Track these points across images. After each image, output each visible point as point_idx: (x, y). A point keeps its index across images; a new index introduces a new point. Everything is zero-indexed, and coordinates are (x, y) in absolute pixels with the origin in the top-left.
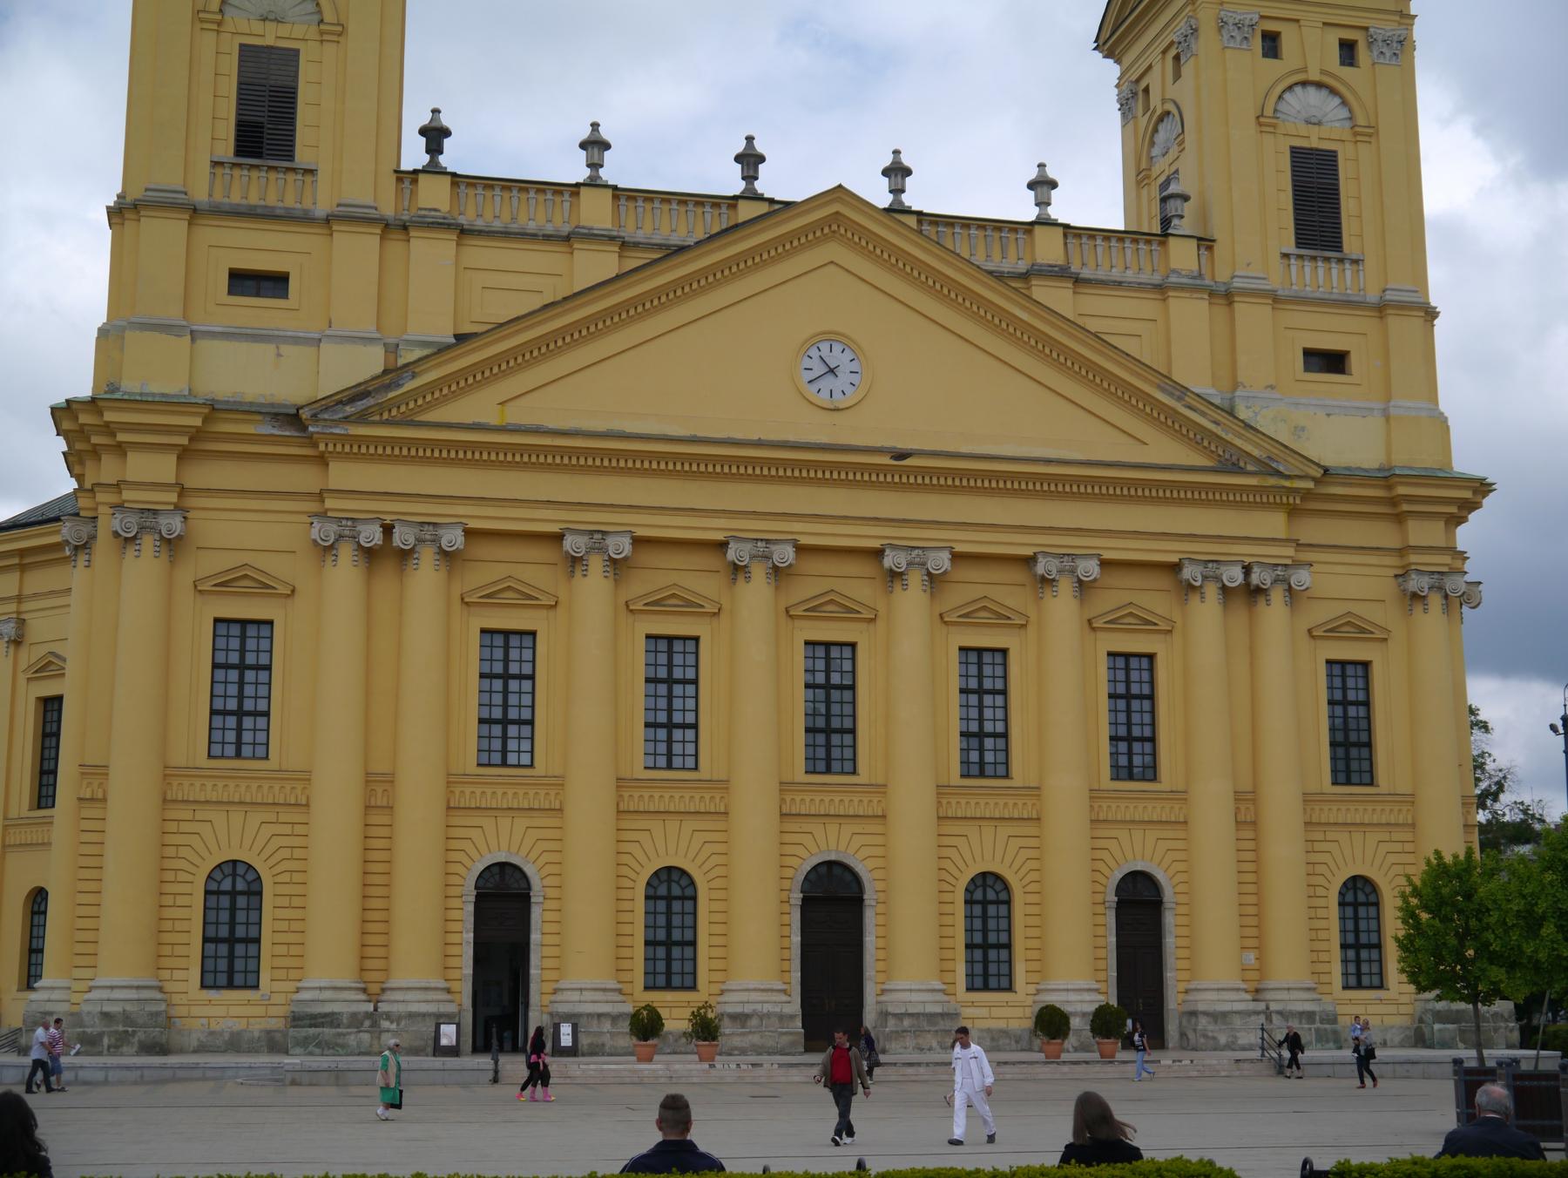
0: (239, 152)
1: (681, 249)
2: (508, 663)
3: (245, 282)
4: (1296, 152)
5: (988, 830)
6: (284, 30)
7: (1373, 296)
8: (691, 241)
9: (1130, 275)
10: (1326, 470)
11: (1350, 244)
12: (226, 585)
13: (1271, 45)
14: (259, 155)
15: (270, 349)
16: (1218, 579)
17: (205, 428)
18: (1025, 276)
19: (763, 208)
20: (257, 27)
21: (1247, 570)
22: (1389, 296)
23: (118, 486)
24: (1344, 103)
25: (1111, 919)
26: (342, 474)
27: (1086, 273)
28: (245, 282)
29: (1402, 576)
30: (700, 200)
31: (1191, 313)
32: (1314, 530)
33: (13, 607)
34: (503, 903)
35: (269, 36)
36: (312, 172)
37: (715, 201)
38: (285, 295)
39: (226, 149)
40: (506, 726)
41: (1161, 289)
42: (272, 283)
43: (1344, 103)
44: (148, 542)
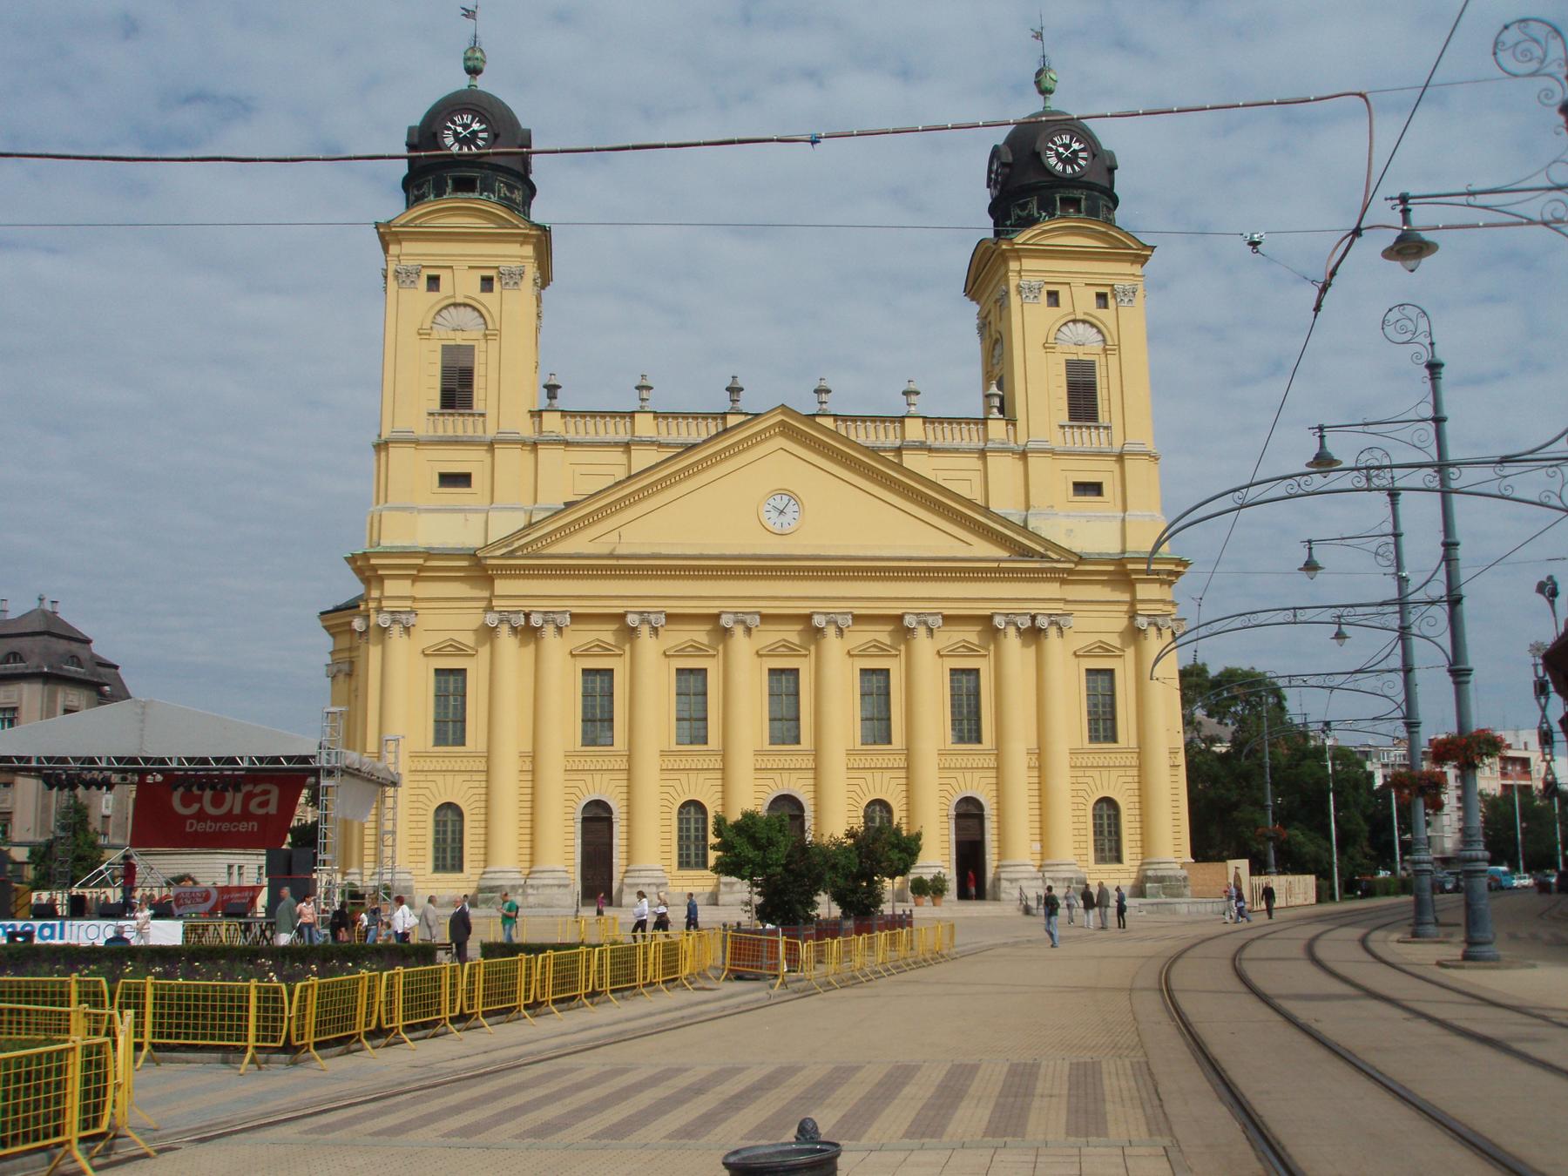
0: (443, 406)
1: (694, 446)
2: (598, 686)
3: (448, 479)
4: (1069, 363)
5: (878, 774)
6: (466, 335)
7: (1117, 448)
8: (699, 440)
9: (965, 444)
10: (1081, 559)
11: (1103, 418)
12: (439, 652)
13: (1053, 298)
14: (453, 407)
15: (461, 516)
16: (1015, 624)
17: (425, 564)
18: (898, 451)
19: (742, 418)
20: (451, 335)
21: (1033, 618)
22: (1127, 448)
23: (379, 600)
24: (1099, 331)
25: (953, 822)
26: (501, 587)
27: (937, 444)
28: (448, 479)
29: (1133, 615)
30: (705, 416)
31: (1003, 468)
32: (1073, 592)
33: (346, 654)
34: (597, 822)
35: (459, 339)
36: (483, 415)
37: (714, 416)
38: (469, 485)
39: (436, 405)
41: (983, 453)
42: (463, 480)
43: (1099, 331)
44: (396, 629)
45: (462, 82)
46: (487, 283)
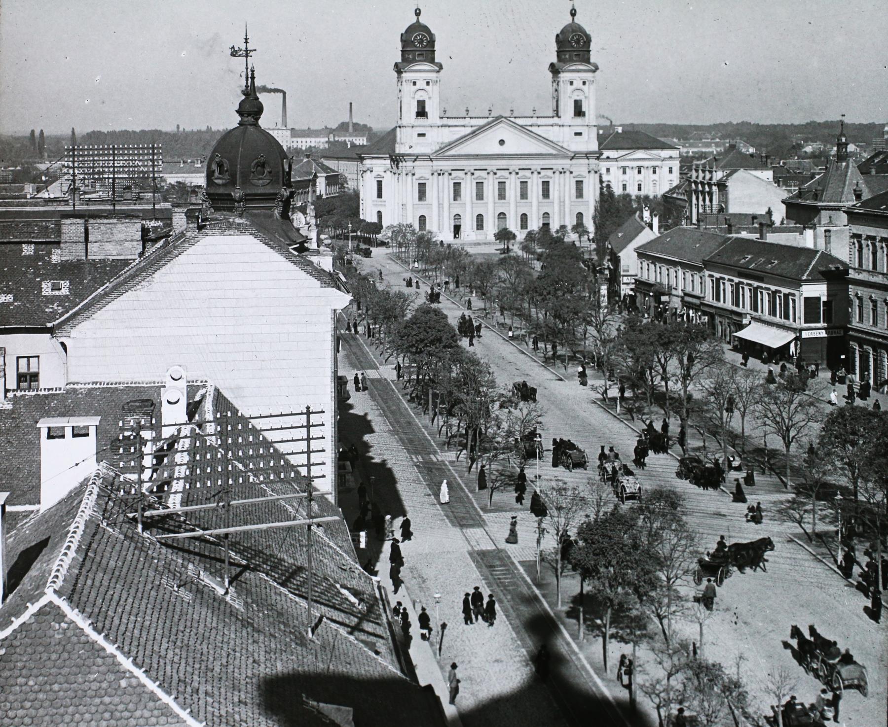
2: (457, 185)
3: (419, 135)
28: (419, 135)
32: (574, 161)
40: (457, 194)
45: (414, 20)
46: (428, 83)
